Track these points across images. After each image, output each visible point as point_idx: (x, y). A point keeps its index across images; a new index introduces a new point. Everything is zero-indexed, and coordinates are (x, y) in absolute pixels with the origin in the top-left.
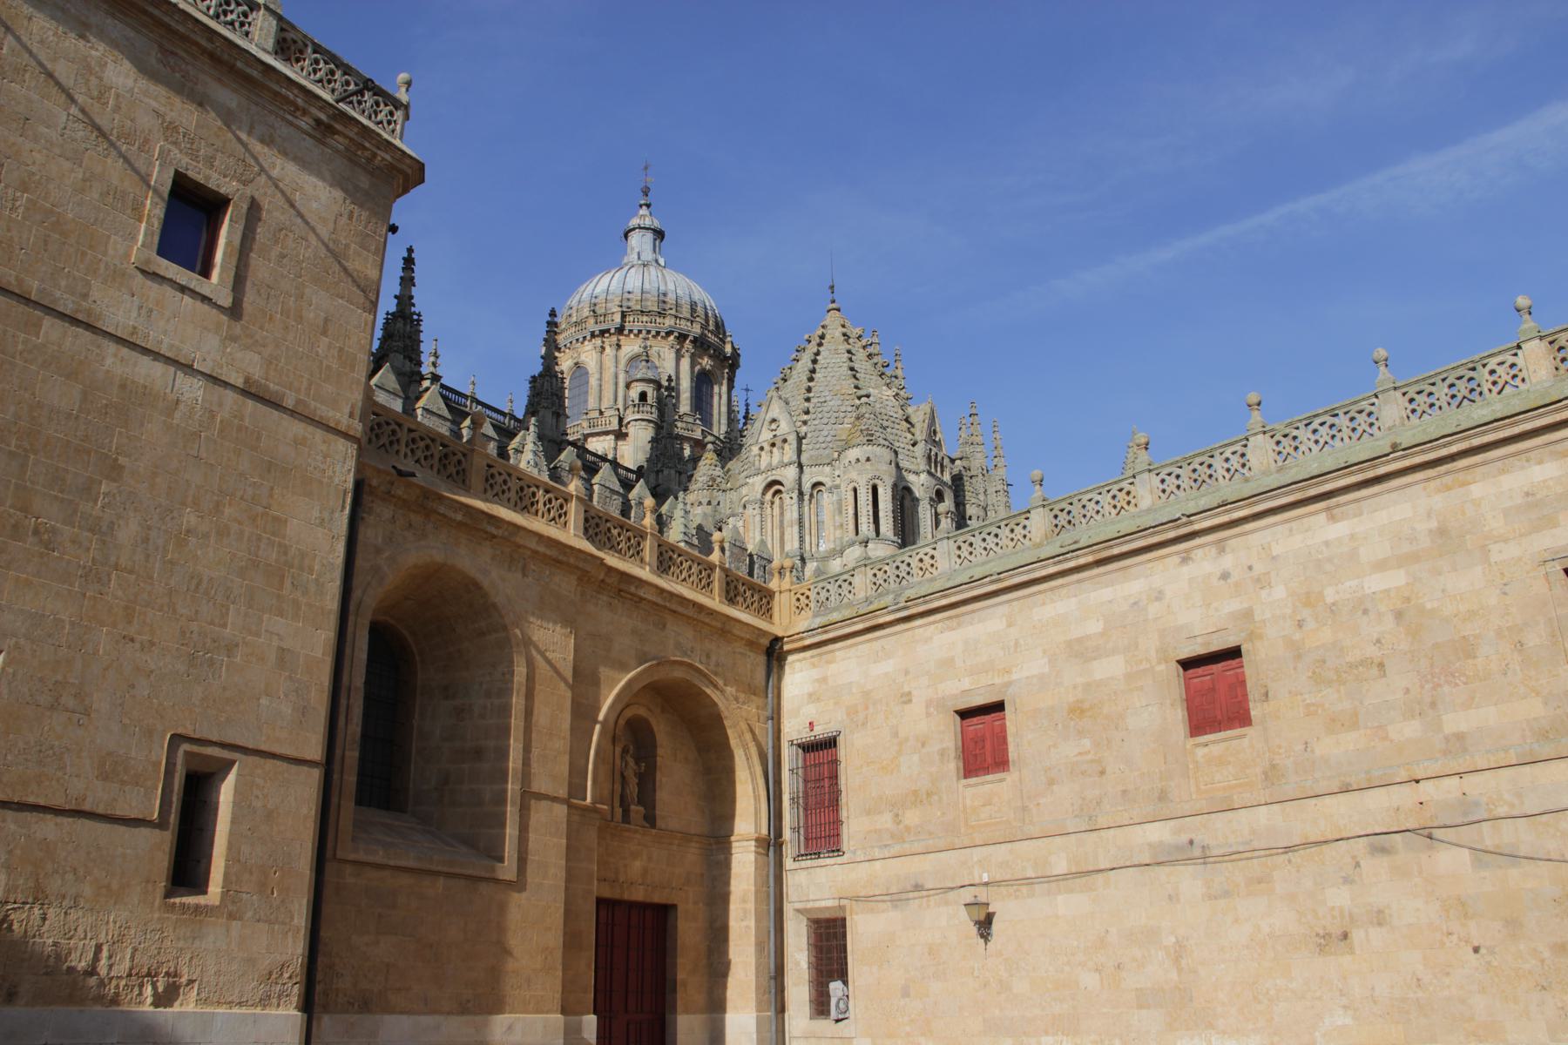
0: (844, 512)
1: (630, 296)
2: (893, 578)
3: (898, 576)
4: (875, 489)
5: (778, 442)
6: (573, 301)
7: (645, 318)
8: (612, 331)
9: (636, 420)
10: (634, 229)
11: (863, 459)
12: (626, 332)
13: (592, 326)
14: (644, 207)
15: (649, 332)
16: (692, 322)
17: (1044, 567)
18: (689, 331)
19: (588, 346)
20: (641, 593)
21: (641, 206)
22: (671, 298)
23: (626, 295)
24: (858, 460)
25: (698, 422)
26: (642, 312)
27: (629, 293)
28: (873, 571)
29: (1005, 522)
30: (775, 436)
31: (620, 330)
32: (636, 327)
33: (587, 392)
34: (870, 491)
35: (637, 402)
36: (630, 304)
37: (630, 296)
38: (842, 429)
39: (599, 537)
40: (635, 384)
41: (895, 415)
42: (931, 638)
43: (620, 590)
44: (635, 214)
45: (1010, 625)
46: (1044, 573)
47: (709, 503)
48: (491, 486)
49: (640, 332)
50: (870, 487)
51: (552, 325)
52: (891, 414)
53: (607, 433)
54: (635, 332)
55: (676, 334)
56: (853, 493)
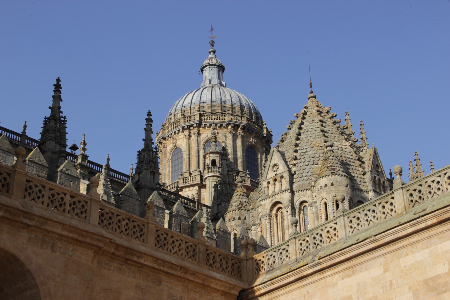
0: (320, 218)
1: (204, 105)
2: (312, 245)
3: (315, 244)
5: (278, 178)
7: (213, 117)
8: (195, 125)
9: (210, 177)
10: (206, 66)
11: (329, 185)
12: (203, 126)
13: (182, 124)
14: (212, 53)
15: (216, 125)
16: (241, 117)
17: (404, 229)
18: (240, 123)
19: (181, 135)
20: (142, 261)
21: (210, 53)
22: (228, 104)
23: (202, 104)
24: (326, 186)
25: (248, 175)
26: (212, 113)
27: (204, 103)
28: (300, 242)
29: (378, 202)
30: (276, 175)
31: (199, 125)
32: (209, 122)
33: (182, 162)
34: (335, 204)
35: (210, 166)
36: (205, 109)
37: (204, 105)
38: (317, 167)
39: (111, 226)
41: (351, 157)
42: (337, 283)
43: (127, 260)
44: (207, 58)
45: (385, 271)
46: (404, 233)
47: (239, 218)
48: (29, 194)
49: (211, 125)
50: (334, 201)
51: (149, 121)
53: (194, 185)
54: (208, 125)
55: (232, 125)
56: (324, 206)
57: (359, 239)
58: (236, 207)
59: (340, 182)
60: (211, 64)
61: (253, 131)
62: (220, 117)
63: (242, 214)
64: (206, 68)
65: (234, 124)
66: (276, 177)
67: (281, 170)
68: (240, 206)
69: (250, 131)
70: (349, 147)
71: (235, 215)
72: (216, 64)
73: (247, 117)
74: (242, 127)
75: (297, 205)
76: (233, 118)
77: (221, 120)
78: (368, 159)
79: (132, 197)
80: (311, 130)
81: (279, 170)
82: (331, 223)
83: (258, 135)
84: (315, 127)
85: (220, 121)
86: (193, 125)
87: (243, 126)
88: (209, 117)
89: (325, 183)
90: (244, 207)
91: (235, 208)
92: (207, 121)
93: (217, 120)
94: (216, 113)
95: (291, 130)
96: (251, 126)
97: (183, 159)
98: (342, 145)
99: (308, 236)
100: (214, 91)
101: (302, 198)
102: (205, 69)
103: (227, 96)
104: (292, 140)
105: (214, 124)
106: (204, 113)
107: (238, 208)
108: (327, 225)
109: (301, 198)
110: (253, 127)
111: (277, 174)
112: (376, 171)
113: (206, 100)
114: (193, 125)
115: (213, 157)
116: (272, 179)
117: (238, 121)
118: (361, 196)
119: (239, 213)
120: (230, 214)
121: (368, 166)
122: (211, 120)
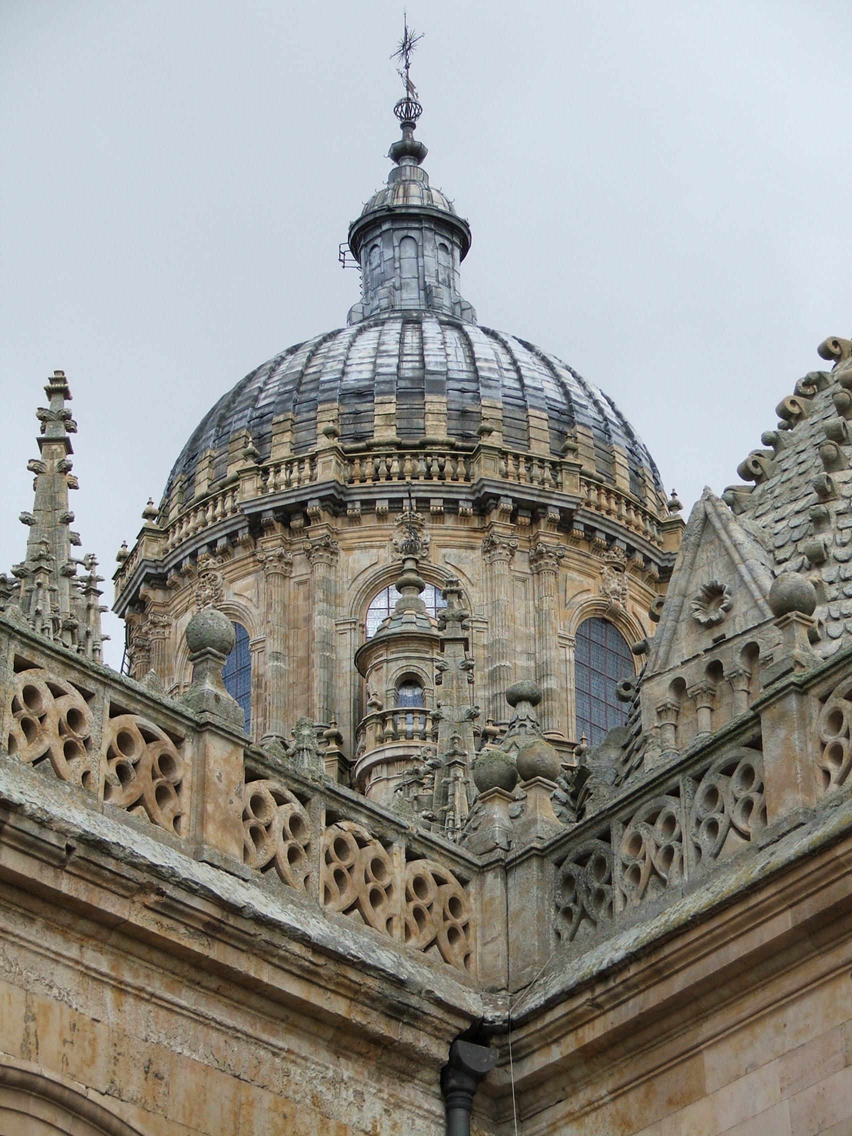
8: (314, 507)
9: (388, 762)
26: (399, 446)
30: (720, 642)
40: (385, 655)
49: (396, 504)
61: (611, 539)
62: (442, 468)
64: (378, 232)
65: (515, 500)
67: (745, 614)
69: (600, 538)
74: (558, 517)
76: (511, 468)
77: (448, 481)
83: (639, 558)
85: (443, 485)
86: (304, 504)
87: (562, 510)
93: (429, 482)
96: (604, 512)
105: (410, 498)
106: (361, 445)
110: (612, 518)
111: (723, 636)
114: (304, 504)
115: (404, 663)
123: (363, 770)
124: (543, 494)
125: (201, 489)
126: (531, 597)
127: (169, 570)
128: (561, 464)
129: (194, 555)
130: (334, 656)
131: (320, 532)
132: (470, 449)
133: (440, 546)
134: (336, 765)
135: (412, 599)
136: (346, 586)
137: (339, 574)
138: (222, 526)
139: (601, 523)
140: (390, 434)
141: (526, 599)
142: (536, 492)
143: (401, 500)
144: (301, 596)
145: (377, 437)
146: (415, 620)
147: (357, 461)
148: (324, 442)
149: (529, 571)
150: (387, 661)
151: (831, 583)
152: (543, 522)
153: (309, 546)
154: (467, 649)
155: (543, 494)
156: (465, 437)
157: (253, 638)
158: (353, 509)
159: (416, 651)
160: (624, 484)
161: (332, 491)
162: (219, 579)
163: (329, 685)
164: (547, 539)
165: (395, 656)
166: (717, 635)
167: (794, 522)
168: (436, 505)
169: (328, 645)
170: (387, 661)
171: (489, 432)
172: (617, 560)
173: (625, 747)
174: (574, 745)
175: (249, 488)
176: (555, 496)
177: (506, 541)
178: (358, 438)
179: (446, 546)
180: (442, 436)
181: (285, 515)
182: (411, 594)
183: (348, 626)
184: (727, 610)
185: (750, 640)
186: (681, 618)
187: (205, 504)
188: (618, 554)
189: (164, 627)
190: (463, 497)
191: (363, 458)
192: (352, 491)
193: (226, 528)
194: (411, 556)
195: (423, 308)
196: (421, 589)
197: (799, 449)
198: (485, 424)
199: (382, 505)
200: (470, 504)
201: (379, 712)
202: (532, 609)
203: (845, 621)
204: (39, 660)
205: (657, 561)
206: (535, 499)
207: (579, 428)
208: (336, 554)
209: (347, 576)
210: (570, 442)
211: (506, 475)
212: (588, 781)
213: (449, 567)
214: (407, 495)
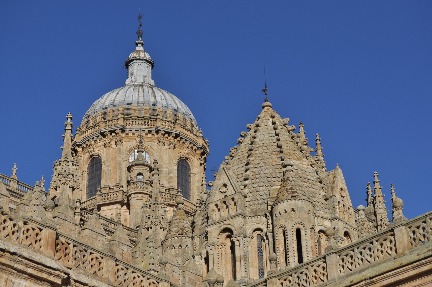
1: (129, 107)
4: (298, 232)
6: (90, 112)
9: (135, 193)
10: (132, 60)
11: (289, 210)
12: (127, 132)
14: (140, 45)
16: (174, 123)
17: (406, 271)
22: (159, 107)
23: (126, 106)
25: (179, 194)
26: (138, 117)
27: (128, 104)
29: (376, 239)
30: (226, 196)
34: (295, 233)
36: (130, 112)
37: (129, 107)
38: (274, 190)
40: (135, 168)
41: (312, 179)
44: (134, 50)
46: (406, 275)
52: (309, 177)
56: (282, 235)
57: (353, 281)
58: (176, 233)
59: (301, 208)
60: (138, 58)
61: (186, 140)
63: (183, 241)
64: (132, 62)
65: (165, 131)
66: (226, 199)
67: (231, 191)
68: (180, 232)
70: (310, 167)
71: (175, 243)
72: (145, 59)
73: (180, 124)
75: (250, 233)
76: (164, 124)
77: (149, 126)
78: (332, 182)
79: (68, 221)
80: (266, 145)
81: (229, 191)
82: (318, 262)
84: (271, 141)
85: (148, 127)
86: (116, 130)
87: (175, 134)
88: (135, 122)
89: (284, 209)
90: (186, 233)
91: (175, 234)
92: (133, 126)
93: (145, 126)
94: (143, 117)
95: (243, 144)
97: (102, 171)
98: (302, 164)
99: (291, 275)
100: (142, 91)
101: (256, 225)
102: (131, 63)
103: (157, 98)
104: (243, 155)
105: (141, 130)
106: (129, 116)
107: (179, 235)
108: (313, 264)
109: (254, 225)
110: (186, 135)
111: (226, 195)
112: (340, 196)
113: (132, 101)
114: (116, 130)
115: (139, 170)
116: (221, 202)
117: (169, 128)
118: (323, 224)
119: (179, 240)
120: (168, 242)
121: (331, 190)
122: (137, 126)
123: (129, 195)
124: (171, 130)
125: (91, 124)
126: (168, 154)
127: (82, 143)
128: (175, 123)
129: (88, 140)
130: (121, 167)
131: (119, 137)
132: (155, 119)
133: (147, 141)
134: (122, 193)
135: (141, 155)
136: (125, 150)
137: (123, 147)
138: (95, 134)
139: (184, 137)
140: (136, 114)
141: (167, 154)
142: (170, 129)
143: (138, 130)
144: (114, 152)
145: (133, 115)
146: (141, 160)
147: (128, 120)
148: (120, 116)
149: (167, 148)
150: (135, 169)
151: (250, 184)
152: (171, 136)
153: (116, 140)
154: (158, 176)
155: (171, 130)
156: (154, 116)
157: (103, 161)
158: (127, 132)
159: (142, 167)
160: (189, 127)
161: (122, 128)
162: (95, 146)
163: (120, 174)
164: (172, 140)
165: (137, 168)
166: (225, 194)
167: (242, 169)
168: (146, 132)
169: (120, 164)
170: (135, 169)
171: (159, 115)
172: (187, 145)
173: (203, 216)
174: (177, 190)
175: (103, 125)
176: (174, 130)
177: (162, 141)
178: (128, 115)
179: (148, 141)
180: (148, 115)
181: (111, 132)
182: (140, 153)
183: (125, 160)
184: (227, 189)
185: (232, 197)
186: (217, 190)
187: (92, 129)
188: (187, 143)
189: (81, 157)
190: (153, 130)
191: (129, 120)
192: (127, 128)
193: (96, 135)
194: (140, 144)
195: (143, 82)
196: (143, 152)
197: (243, 150)
198: (159, 113)
199: (134, 131)
200: (154, 132)
201: (133, 182)
202: (168, 157)
203: (253, 193)
204: (136, 271)
205: (197, 145)
206: (169, 131)
207: (179, 114)
208: (123, 143)
209: (125, 148)
210: (178, 118)
211: (162, 125)
212: (195, 224)
213: (149, 146)
214: (140, 129)
